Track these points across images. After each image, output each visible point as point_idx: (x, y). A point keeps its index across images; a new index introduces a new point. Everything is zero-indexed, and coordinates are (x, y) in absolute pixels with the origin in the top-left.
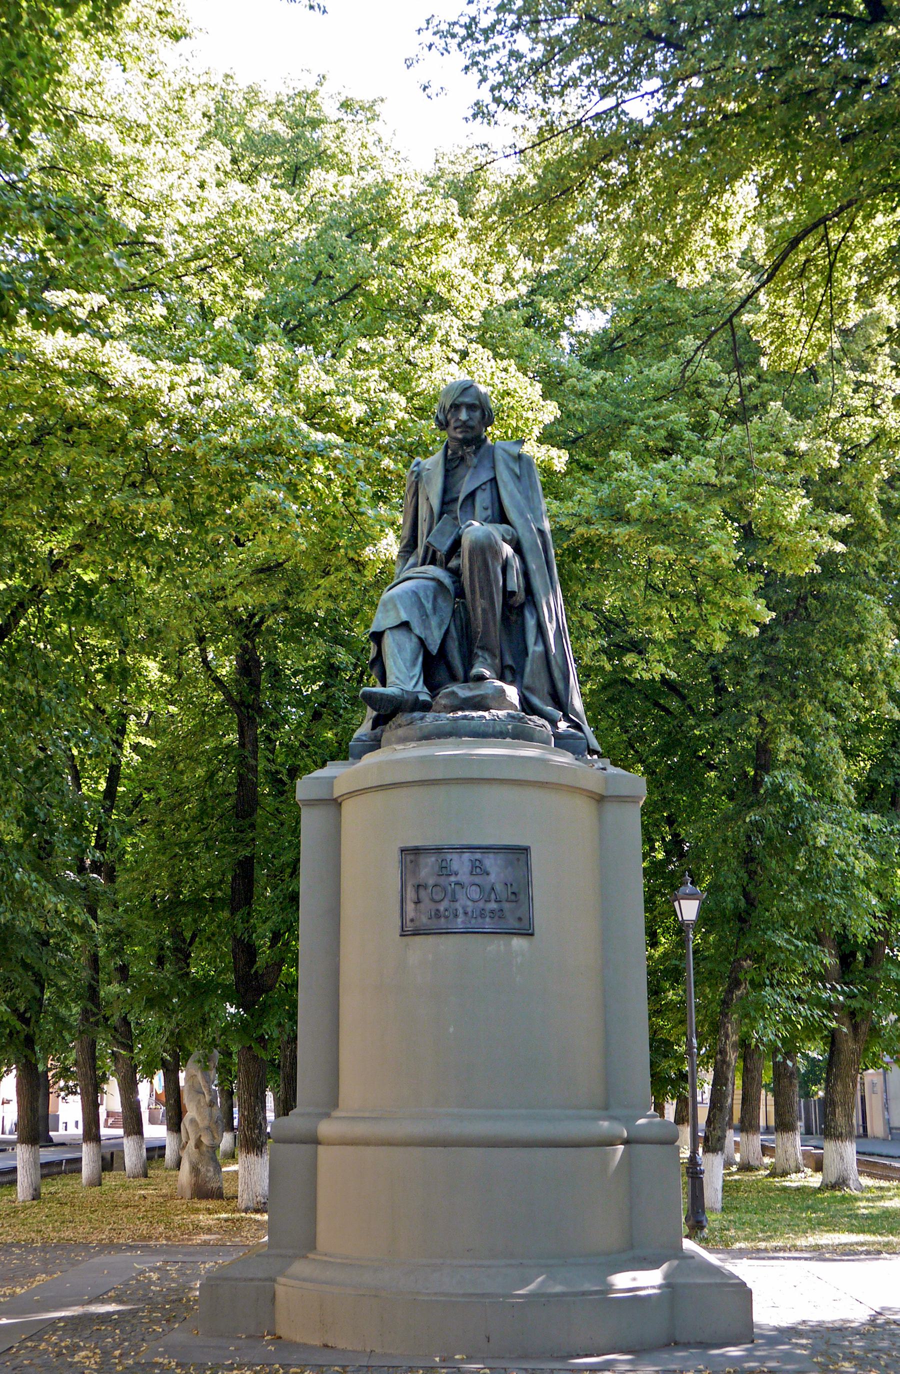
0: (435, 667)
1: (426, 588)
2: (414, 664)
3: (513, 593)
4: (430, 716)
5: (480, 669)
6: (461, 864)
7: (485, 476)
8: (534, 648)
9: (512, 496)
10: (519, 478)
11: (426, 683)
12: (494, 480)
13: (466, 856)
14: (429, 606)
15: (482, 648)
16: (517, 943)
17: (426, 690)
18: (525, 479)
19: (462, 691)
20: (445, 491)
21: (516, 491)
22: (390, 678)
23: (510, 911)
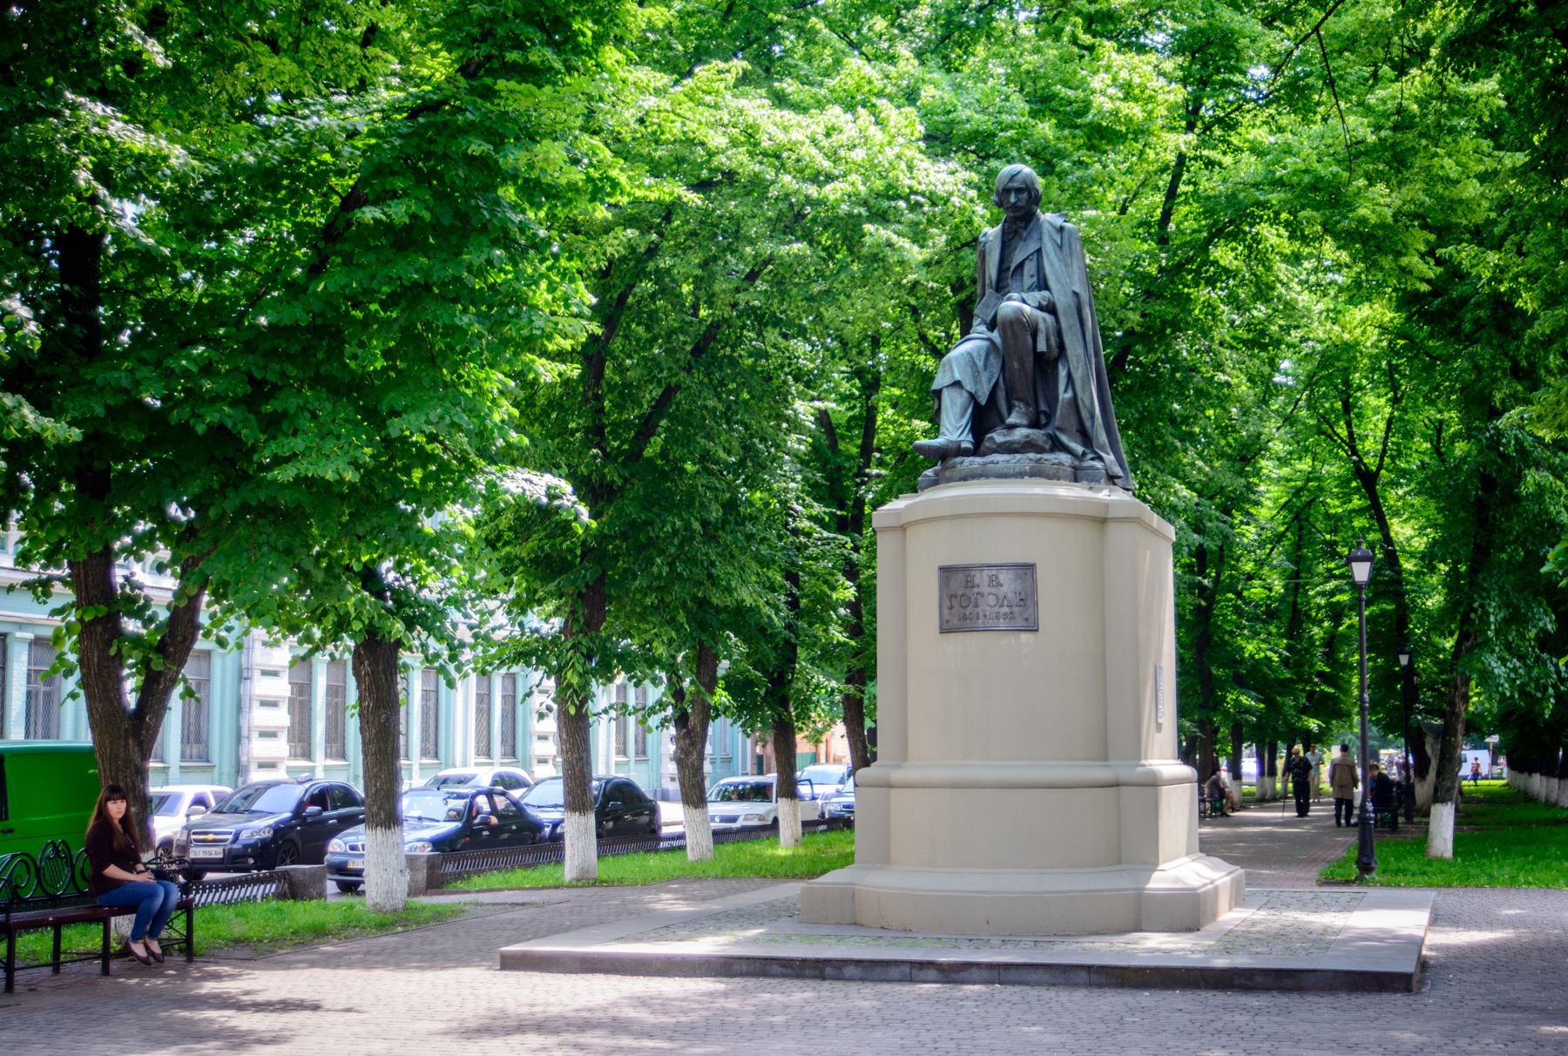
0: (983, 418)
1: (979, 349)
2: (963, 416)
3: (1042, 353)
4: (968, 460)
5: (1011, 420)
6: (982, 579)
7: (1032, 247)
8: (1064, 395)
9: (1052, 265)
10: (1061, 247)
11: (972, 430)
12: (1039, 251)
13: (986, 573)
14: (980, 364)
15: (1019, 400)
16: (1024, 637)
17: (970, 438)
18: (1066, 248)
19: (998, 437)
20: (1002, 260)
21: (1055, 261)
22: (943, 430)
23: (1024, 614)
